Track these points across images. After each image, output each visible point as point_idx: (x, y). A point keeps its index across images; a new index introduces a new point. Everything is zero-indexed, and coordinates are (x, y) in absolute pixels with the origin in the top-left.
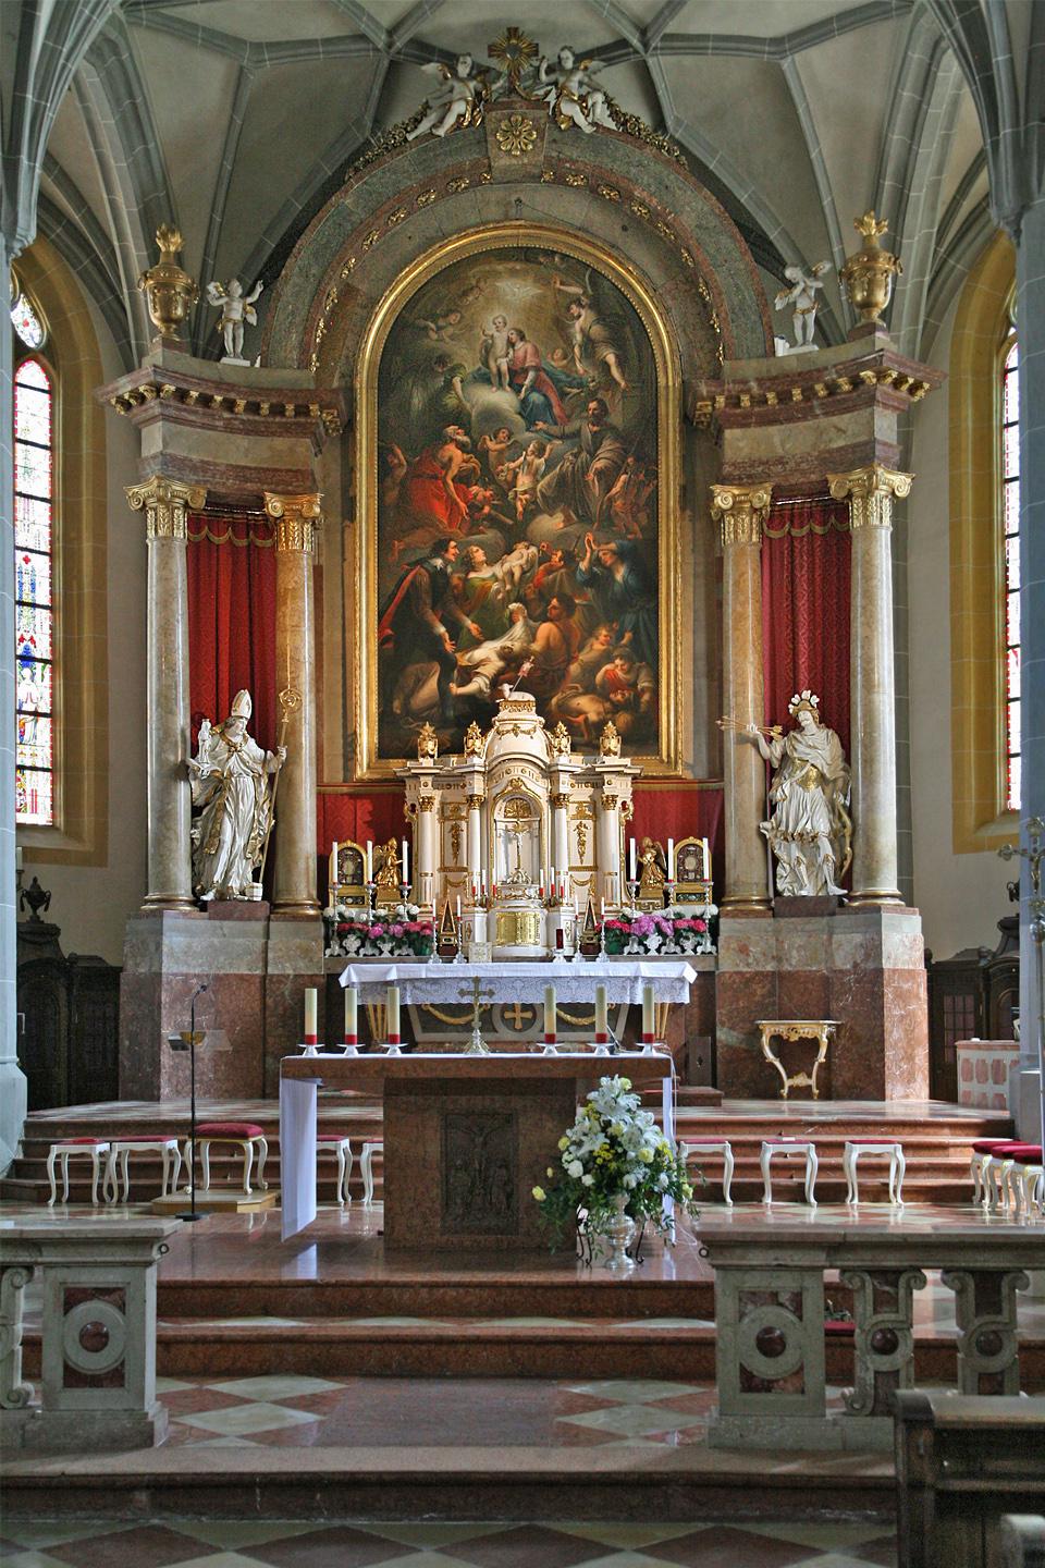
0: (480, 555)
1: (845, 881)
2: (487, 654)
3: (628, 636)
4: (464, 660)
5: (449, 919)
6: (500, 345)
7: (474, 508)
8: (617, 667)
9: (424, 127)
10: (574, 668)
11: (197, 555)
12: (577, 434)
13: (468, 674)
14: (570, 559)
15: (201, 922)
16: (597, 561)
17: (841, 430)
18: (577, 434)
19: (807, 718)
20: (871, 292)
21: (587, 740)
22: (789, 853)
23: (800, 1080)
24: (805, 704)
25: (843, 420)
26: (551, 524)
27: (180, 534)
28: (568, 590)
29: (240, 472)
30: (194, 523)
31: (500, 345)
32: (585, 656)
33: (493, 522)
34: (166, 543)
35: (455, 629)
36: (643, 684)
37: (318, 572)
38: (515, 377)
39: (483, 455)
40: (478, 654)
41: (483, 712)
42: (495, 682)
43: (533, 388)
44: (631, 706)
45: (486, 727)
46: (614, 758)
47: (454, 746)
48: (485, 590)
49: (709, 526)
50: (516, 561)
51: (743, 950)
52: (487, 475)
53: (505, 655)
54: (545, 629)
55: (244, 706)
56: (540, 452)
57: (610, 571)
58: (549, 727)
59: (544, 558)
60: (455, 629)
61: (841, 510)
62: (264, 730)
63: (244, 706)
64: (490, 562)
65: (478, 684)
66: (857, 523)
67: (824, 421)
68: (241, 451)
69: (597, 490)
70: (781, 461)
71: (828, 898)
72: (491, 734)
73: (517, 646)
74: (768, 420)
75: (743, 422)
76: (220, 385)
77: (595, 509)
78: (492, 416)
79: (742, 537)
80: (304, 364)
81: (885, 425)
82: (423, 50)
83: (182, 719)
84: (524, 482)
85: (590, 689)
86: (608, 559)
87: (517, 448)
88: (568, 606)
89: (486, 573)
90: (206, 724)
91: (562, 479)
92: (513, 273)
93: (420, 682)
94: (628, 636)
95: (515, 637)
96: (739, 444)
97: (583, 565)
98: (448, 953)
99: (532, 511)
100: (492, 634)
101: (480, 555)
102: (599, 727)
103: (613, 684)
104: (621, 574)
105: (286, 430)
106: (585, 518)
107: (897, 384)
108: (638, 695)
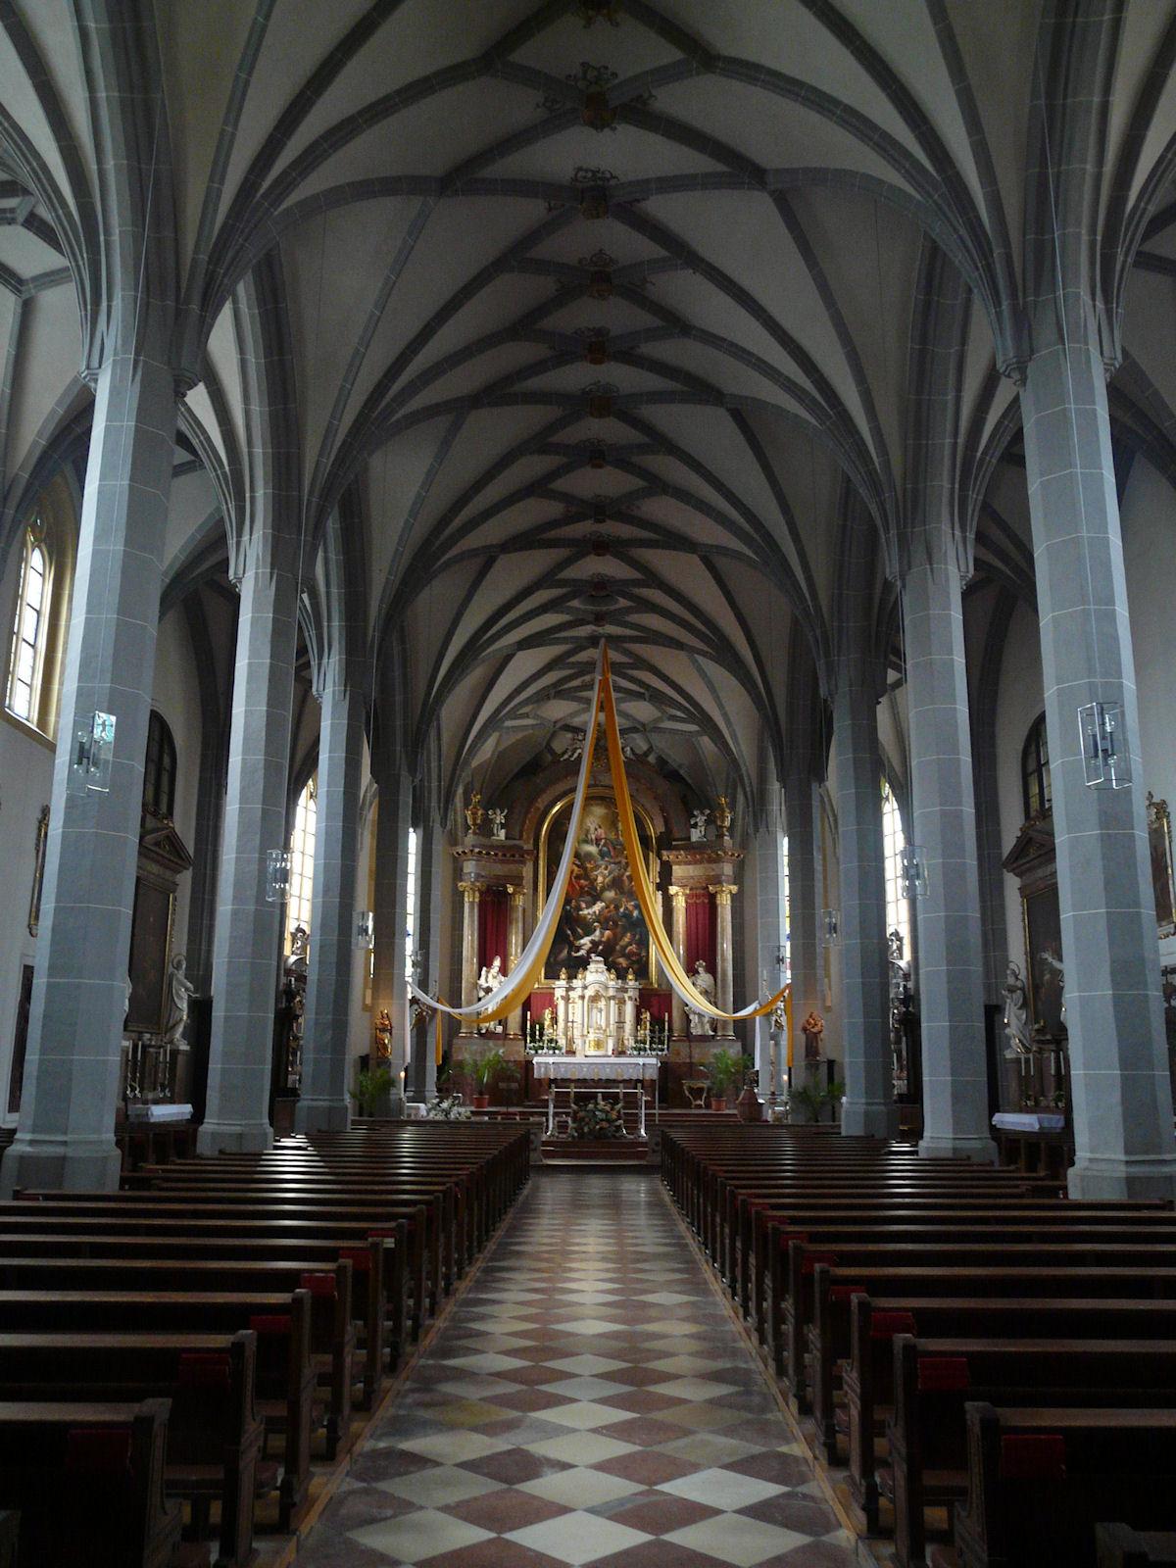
0: (584, 905)
1: (715, 1030)
2: (586, 941)
3: (637, 937)
4: (577, 943)
5: (570, 1041)
6: (592, 830)
7: (582, 887)
8: (633, 948)
9: (566, 757)
10: (618, 948)
11: (482, 905)
12: (620, 862)
13: (578, 949)
14: (617, 908)
15: (482, 1041)
16: (626, 909)
17: (713, 869)
18: (620, 862)
19: (701, 970)
20: (723, 821)
21: (621, 975)
22: (694, 1019)
23: (699, 1102)
24: (701, 965)
25: (714, 866)
26: (610, 894)
27: (477, 900)
28: (616, 918)
29: (497, 877)
30: (481, 894)
31: (592, 830)
32: (622, 943)
33: (589, 894)
34: (472, 904)
35: (574, 932)
36: (643, 954)
37: (524, 909)
38: (597, 841)
39: (585, 869)
40: (582, 941)
41: (584, 963)
42: (589, 952)
43: (604, 845)
44: (638, 962)
45: (585, 969)
46: (632, 982)
47: (571, 977)
48: (585, 918)
49: (668, 901)
50: (598, 907)
51: (679, 1054)
52: (586, 877)
53: (592, 942)
54: (607, 932)
55: (497, 963)
56: (606, 869)
57: (632, 912)
58: (609, 970)
59: (607, 907)
60: (574, 932)
61: (712, 897)
62: (504, 971)
63: (497, 963)
64: (587, 908)
65: (582, 952)
66: (718, 902)
67: (706, 865)
68: (500, 869)
69: (627, 882)
70: (692, 877)
71: (708, 1036)
72: (588, 973)
73: (597, 939)
74: (686, 863)
75: (679, 863)
76: (492, 847)
77: (626, 889)
78: (589, 855)
79: (680, 903)
80: (521, 838)
81: (728, 869)
82: (567, 728)
83: (475, 967)
84: (600, 879)
85: (623, 956)
86: (631, 908)
87: (597, 867)
88: (615, 923)
89: (586, 912)
90: (484, 969)
91: (614, 879)
92: (597, 805)
93: (561, 952)
94: (637, 937)
95: (597, 935)
96: (678, 871)
97: (622, 910)
98: (571, 1052)
99: (603, 889)
100: (588, 935)
101: (584, 905)
102: (626, 971)
103: (632, 953)
104: (636, 913)
105: (516, 862)
106: (622, 893)
107: (733, 855)
108: (641, 958)
